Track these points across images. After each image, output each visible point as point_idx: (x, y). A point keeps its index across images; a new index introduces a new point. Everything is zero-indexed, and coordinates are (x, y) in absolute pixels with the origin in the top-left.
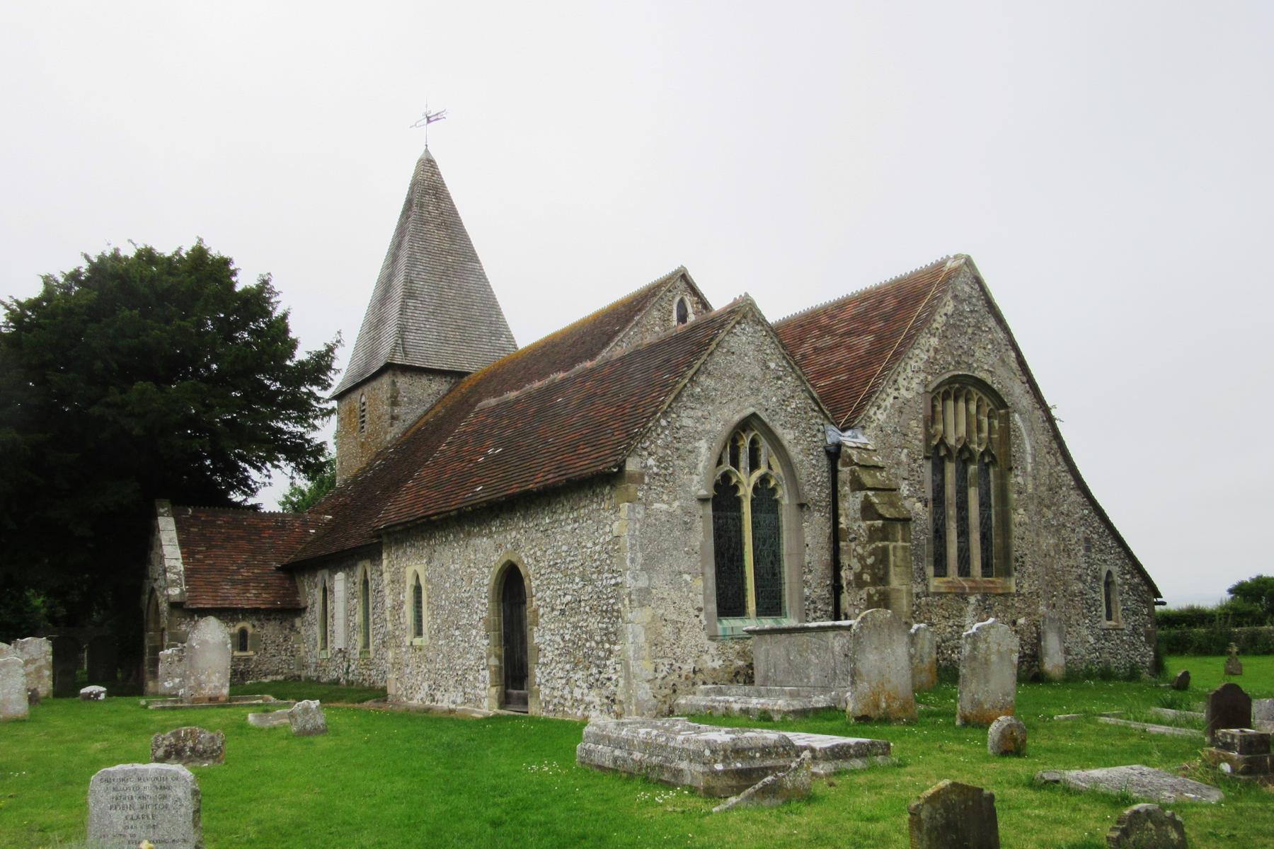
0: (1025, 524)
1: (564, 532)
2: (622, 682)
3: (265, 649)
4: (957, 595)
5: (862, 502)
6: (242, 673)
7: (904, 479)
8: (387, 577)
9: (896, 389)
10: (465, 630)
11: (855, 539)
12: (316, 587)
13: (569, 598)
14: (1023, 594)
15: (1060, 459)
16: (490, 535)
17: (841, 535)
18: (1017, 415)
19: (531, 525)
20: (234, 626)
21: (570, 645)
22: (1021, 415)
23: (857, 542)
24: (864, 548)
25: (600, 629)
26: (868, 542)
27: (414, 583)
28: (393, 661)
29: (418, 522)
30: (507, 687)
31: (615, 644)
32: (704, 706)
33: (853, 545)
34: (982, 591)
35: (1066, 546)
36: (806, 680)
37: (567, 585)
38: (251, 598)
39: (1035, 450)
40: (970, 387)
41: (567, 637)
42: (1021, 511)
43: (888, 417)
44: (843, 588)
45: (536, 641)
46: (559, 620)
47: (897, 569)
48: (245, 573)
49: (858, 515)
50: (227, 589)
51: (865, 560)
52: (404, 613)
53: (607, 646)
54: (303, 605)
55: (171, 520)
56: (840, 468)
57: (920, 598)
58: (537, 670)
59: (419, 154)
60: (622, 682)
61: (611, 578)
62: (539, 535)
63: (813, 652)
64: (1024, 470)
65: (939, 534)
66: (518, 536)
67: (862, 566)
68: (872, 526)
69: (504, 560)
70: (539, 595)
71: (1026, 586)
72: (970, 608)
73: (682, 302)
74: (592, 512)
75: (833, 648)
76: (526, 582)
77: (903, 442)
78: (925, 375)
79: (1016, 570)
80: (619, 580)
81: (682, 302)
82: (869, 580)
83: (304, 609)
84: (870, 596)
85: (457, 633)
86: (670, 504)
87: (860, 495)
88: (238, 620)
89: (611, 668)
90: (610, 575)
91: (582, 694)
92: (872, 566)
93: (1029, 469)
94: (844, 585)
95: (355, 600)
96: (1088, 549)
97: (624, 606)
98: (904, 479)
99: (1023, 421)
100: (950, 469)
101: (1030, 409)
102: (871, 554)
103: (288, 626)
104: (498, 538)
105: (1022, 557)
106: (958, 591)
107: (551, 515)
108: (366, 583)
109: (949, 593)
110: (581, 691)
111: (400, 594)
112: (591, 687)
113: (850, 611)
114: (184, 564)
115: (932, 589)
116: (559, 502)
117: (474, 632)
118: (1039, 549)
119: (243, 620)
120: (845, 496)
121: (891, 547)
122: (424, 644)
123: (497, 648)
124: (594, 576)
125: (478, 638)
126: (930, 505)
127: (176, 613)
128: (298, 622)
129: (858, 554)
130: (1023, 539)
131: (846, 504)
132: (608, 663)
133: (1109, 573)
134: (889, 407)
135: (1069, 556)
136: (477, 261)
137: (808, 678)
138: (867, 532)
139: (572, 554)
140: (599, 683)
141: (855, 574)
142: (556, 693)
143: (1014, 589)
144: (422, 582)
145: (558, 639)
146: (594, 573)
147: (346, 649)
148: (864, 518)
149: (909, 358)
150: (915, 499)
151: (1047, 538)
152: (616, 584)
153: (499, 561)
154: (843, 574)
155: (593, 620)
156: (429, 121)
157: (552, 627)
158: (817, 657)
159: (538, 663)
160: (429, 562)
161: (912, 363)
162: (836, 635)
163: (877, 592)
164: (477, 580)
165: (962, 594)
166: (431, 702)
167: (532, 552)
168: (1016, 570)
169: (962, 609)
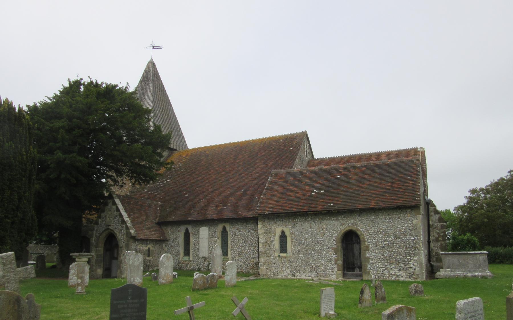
1: (383, 222)
2: (417, 269)
3: (155, 256)
5: (439, 218)
6: (148, 266)
8: (260, 231)
10: (319, 253)
11: (436, 228)
12: (179, 231)
13: (388, 242)
16: (337, 220)
17: (430, 226)
19: (363, 218)
20: (147, 246)
21: (387, 257)
23: (436, 229)
24: (439, 230)
25: (405, 252)
26: (440, 229)
27: (281, 234)
28: (264, 262)
29: (298, 213)
30: (344, 270)
31: (414, 257)
32: (454, 275)
33: (435, 229)
36: (467, 268)
37: (385, 238)
38: (153, 235)
41: (386, 255)
44: (430, 241)
45: (367, 255)
46: (380, 249)
48: (148, 225)
49: (437, 221)
50: (147, 232)
51: (440, 234)
52: (274, 245)
53: (409, 258)
54: (168, 239)
55: (118, 200)
56: (430, 207)
58: (368, 266)
59: (149, 59)
60: (417, 269)
61: (411, 237)
62: (369, 222)
63: (470, 260)
66: (355, 222)
67: (439, 236)
68: (443, 224)
69: (348, 229)
70: (369, 241)
73: (306, 142)
74: (401, 216)
75: (479, 259)
76: (361, 237)
80: (416, 238)
81: (306, 142)
82: (441, 239)
83: (169, 240)
84: (441, 244)
85: (312, 252)
87: (438, 216)
88: (148, 244)
89: (411, 264)
90: (411, 236)
91: (395, 272)
92: (442, 236)
94: (431, 240)
95: (215, 238)
97: (419, 246)
102: (442, 233)
103: (161, 247)
104: (343, 222)
107: (375, 216)
108: (224, 232)
110: (394, 272)
111: (271, 238)
112: (400, 270)
113: (434, 248)
114: (130, 219)
116: (381, 212)
117: (325, 252)
119: (149, 244)
120: (432, 215)
122: (288, 256)
123: (341, 258)
124: (402, 236)
125: (328, 254)
127: (131, 240)
128: (164, 245)
129: (437, 232)
131: (432, 218)
132: (410, 263)
136: (171, 106)
137: (468, 267)
138: (441, 226)
139: (389, 229)
140: (405, 269)
141: (436, 238)
142: (379, 272)
144: (287, 233)
145: (380, 255)
146: (401, 235)
147: (208, 257)
148: (439, 222)
152: (415, 239)
153: (344, 229)
154: (431, 238)
155: (401, 250)
156: (153, 48)
157: (377, 251)
158: (472, 261)
159: (369, 263)
160: (293, 227)
162: (481, 255)
163: (444, 243)
164: (328, 235)
166: (293, 276)
167: (364, 227)
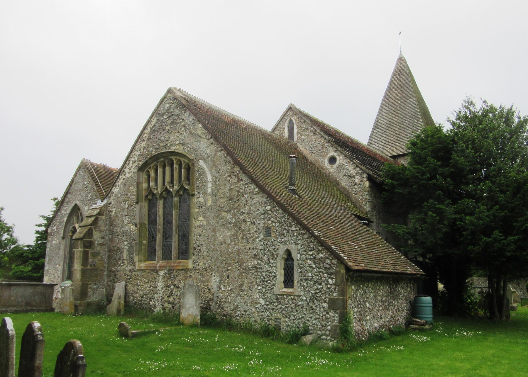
0: (203, 225)
4: (151, 270)
7: (126, 216)
9: (124, 175)
14: (199, 269)
15: (243, 176)
18: (201, 161)
22: (204, 160)
34: (168, 268)
35: (244, 235)
39: (216, 178)
40: (171, 157)
42: (201, 218)
43: (120, 189)
47: (77, 260)
57: (131, 272)
64: (205, 193)
65: (152, 238)
71: (201, 264)
72: (160, 278)
77: (125, 198)
78: (138, 162)
79: (194, 254)
86: (56, 241)
93: (209, 190)
96: (268, 234)
98: (126, 216)
99: (206, 163)
100: (160, 203)
101: (213, 155)
105: (199, 247)
106: (152, 268)
109: (147, 270)
115: (137, 268)
118: (215, 240)
121: (76, 251)
126: (138, 226)
130: (200, 235)
133: (288, 253)
134: (120, 185)
135: (248, 242)
143: (190, 266)
149: (130, 158)
150: (131, 224)
151: (223, 232)
161: (133, 159)
165: (154, 270)
168: (194, 254)
169: (155, 278)
